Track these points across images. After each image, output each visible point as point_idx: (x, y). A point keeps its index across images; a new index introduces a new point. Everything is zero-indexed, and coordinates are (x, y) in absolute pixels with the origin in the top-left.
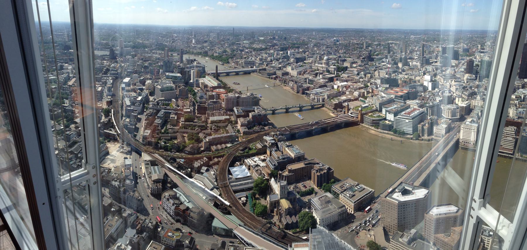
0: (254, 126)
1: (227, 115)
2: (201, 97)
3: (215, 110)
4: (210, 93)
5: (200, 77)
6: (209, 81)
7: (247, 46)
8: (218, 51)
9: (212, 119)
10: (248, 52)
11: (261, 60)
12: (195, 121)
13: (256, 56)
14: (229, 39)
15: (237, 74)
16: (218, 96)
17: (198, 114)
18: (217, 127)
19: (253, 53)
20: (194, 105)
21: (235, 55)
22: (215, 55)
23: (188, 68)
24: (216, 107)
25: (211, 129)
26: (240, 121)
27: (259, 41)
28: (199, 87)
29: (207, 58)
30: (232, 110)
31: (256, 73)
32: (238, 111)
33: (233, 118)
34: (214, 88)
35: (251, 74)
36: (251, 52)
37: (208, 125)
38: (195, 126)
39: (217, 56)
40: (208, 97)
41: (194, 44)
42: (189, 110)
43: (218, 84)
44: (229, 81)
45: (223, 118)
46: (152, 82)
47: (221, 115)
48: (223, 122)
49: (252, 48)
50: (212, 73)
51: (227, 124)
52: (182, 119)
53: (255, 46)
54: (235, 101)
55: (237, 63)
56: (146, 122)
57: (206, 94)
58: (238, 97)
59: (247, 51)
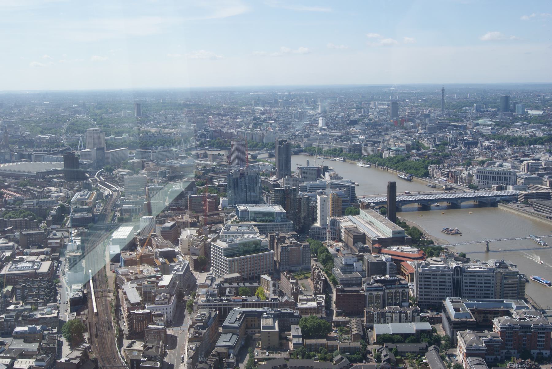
0: (508, 358)
1: (423, 320)
2: (348, 268)
3: (390, 305)
4: (373, 257)
5: (343, 213)
6: (370, 223)
7: (487, 131)
8: (394, 144)
9: (379, 329)
10: (489, 148)
11: (531, 169)
12: (333, 334)
13: (516, 158)
14: (427, 116)
15: (454, 205)
16: (397, 264)
17: (338, 314)
18: (396, 353)
19: (508, 150)
20: (327, 290)
21: (447, 156)
22: (386, 154)
23: (304, 189)
24: (392, 296)
25: (378, 359)
26: (464, 340)
27: (526, 119)
28: (341, 240)
29: (360, 164)
30: (440, 308)
31: (515, 206)
32: (457, 310)
33: (442, 331)
34: (384, 243)
35: (500, 207)
36: (501, 148)
37: (369, 348)
38: (332, 349)
39: (390, 159)
40: (366, 267)
41: (321, 129)
42: (314, 304)
43: (394, 233)
44: (431, 227)
45: (412, 327)
46: (200, 233)
47: (407, 320)
48: (413, 341)
49: (503, 138)
50: (377, 203)
51: (423, 345)
52: (295, 330)
53: (511, 132)
54: (449, 280)
55: (454, 177)
56: (193, 346)
57: (361, 258)
58: (458, 271)
59: (486, 144)
